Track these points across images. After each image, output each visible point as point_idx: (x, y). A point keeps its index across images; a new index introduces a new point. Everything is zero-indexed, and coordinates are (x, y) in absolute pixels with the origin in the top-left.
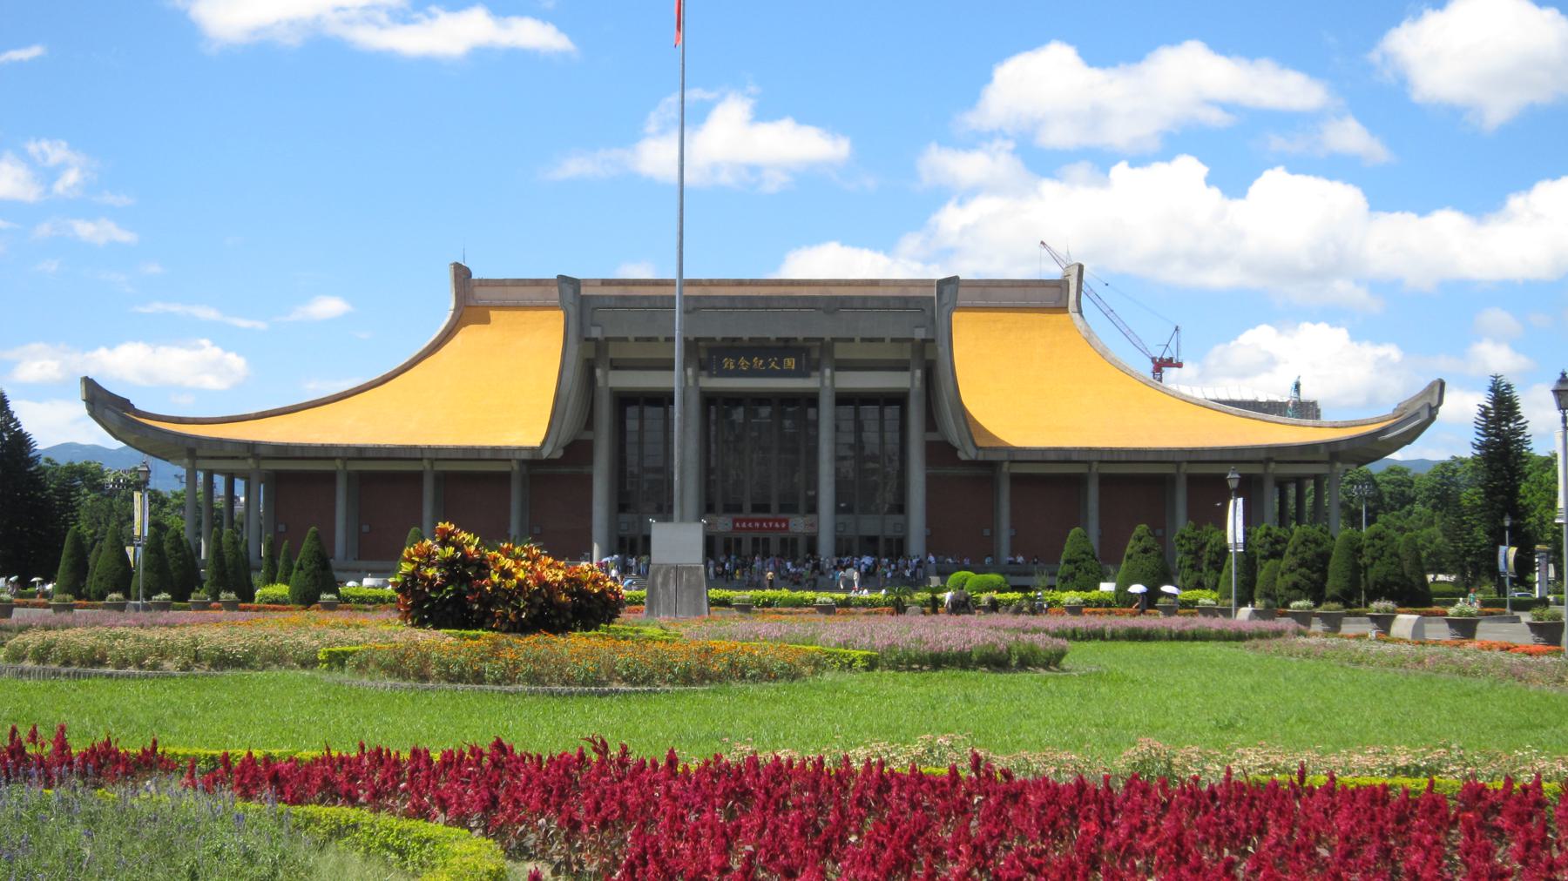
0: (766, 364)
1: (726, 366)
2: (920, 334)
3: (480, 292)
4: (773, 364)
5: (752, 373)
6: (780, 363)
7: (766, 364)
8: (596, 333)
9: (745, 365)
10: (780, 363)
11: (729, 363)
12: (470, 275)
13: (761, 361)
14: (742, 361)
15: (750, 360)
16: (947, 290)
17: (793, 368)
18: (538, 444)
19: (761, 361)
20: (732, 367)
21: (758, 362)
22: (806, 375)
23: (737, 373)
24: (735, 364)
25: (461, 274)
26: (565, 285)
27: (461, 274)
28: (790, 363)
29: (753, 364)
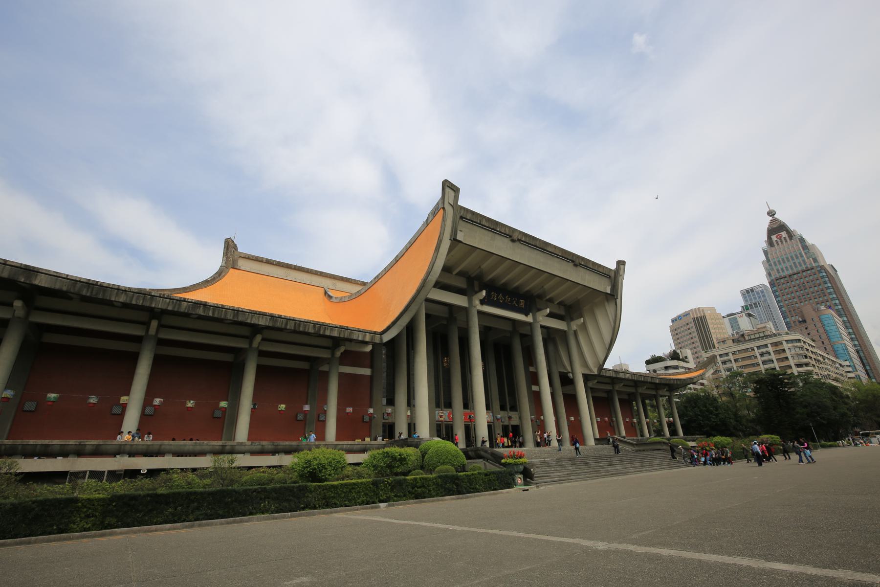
0: (511, 301)
1: (492, 298)
3: (242, 263)
4: (515, 302)
6: (518, 303)
7: (511, 301)
9: (502, 299)
13: (509, 299)
15: (504, 296)
16: (622, 267)
17: (523, 307)
18: (380, 330)
19: (509, 299)
20: (496, 299)
24: (497, 297)
26: (448, 190)
29: (505, 299)
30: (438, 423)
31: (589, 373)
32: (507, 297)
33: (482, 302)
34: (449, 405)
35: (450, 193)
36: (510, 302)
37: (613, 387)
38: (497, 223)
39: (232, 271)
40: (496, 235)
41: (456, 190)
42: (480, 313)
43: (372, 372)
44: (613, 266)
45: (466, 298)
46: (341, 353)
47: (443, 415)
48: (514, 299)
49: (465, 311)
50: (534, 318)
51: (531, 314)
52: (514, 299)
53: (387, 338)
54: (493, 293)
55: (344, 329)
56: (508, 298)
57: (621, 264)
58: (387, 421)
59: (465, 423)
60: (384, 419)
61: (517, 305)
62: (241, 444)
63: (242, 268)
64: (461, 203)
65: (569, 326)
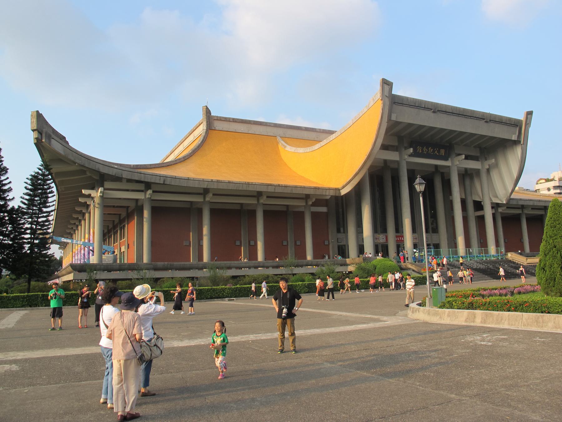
0: (434, 151)
1: (418, 151)
2: (514, 138)
6: (439, 152)
7: (434, 151)
9: (426, 151)
12: (210, 114)
14: (425, 149)
15: (427, 148)
17: (443, 155)
19: (432, 150)
20: (421, 151)
22: (446, 159)
25: (208, 112)
27: (208, 112)
28: (443, 152)
29: (429, 150)
30: (377, 244)
31: (500, 202)
32: (430, 148)
33: (411, 155)
34: (384, 230)
35: (387, 87)
36: (432, 152)
37: (522, 211)
38: (421, 102)
39: (210, 132)
40: (421, 110)
42: (408, 163)
43: (328, 210)
44: (521, 116)
45: (397, 153)
46: (312, 203)
47: (381, 239)
48: (435, 149)
49: (398, 162)
50: (452, 163)
51: (450, 159)
52: (435, 149)
53: (343, 192)
54: (419, 147)
55: (317, 189)
56: (431, 149)
57: (529, 114)
58: (340, 244)
59: (397, 243)
60: (338, 242)
61: (438, 154)
62: (260, 262)
63: (217, 128)
64: (394, 92)
65: (482, 164)
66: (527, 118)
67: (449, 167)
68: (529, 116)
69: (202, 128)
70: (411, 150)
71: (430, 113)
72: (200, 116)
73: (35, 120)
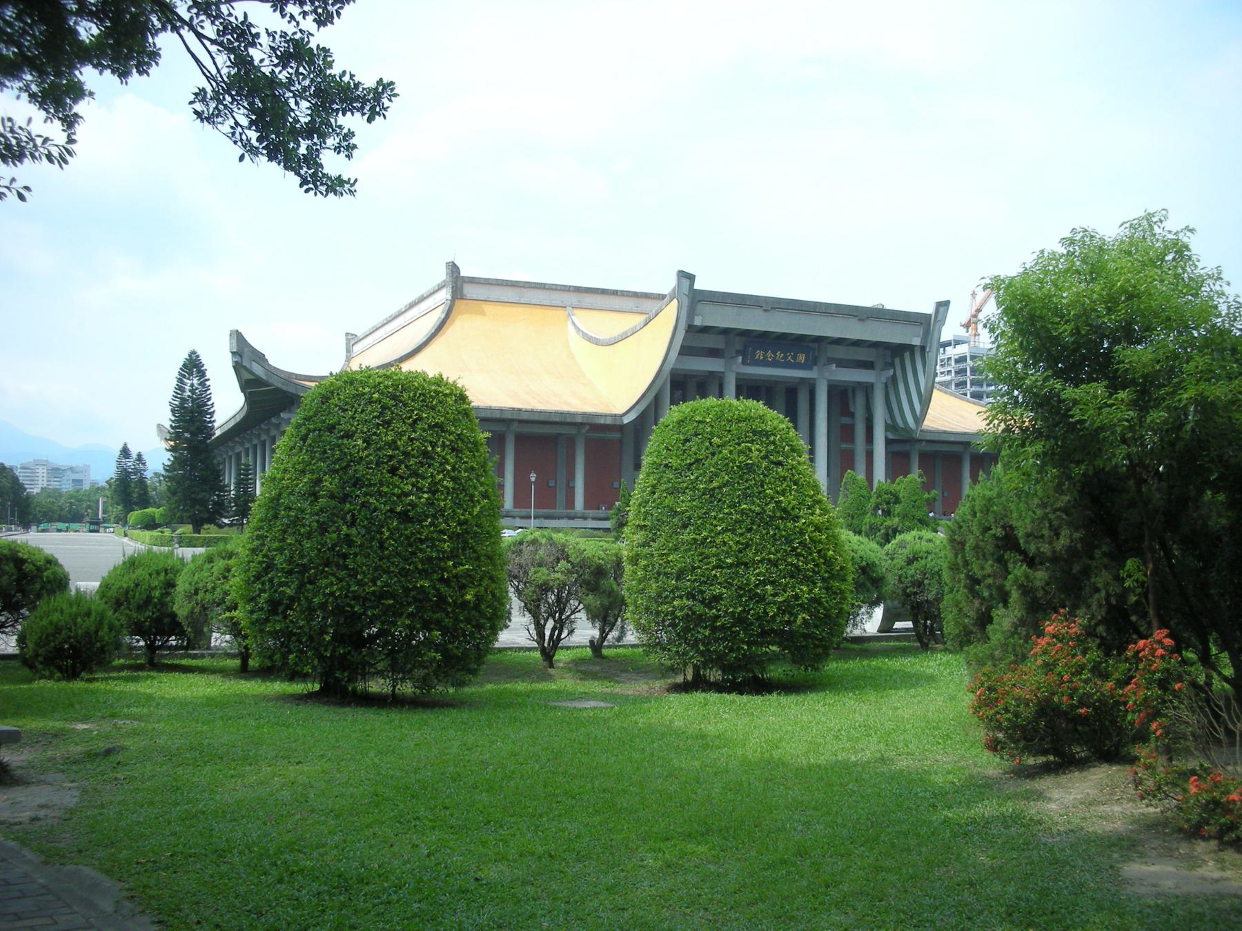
2: (916, 341)
3: (469, 290)
5: (775, 364)
6: (794, 357)
8: (698, 321)
10: (794, 357)
11: (759, 355)
14: (769, 353)
15: (774, 353)
16: (942, 309)
21: (780, 355)
23: (765, 363)
28: (802, 358)
35: (686, 283)
41: (691, 278)
44: (929, 309)
53: (626, 420)
66: (937, 311)
67: (815, 379)
68: (942, 309)
69: (445, 295)
70: (740, 359)
71: (758, 312)
72: (442, 275)
73: (234, 341)
